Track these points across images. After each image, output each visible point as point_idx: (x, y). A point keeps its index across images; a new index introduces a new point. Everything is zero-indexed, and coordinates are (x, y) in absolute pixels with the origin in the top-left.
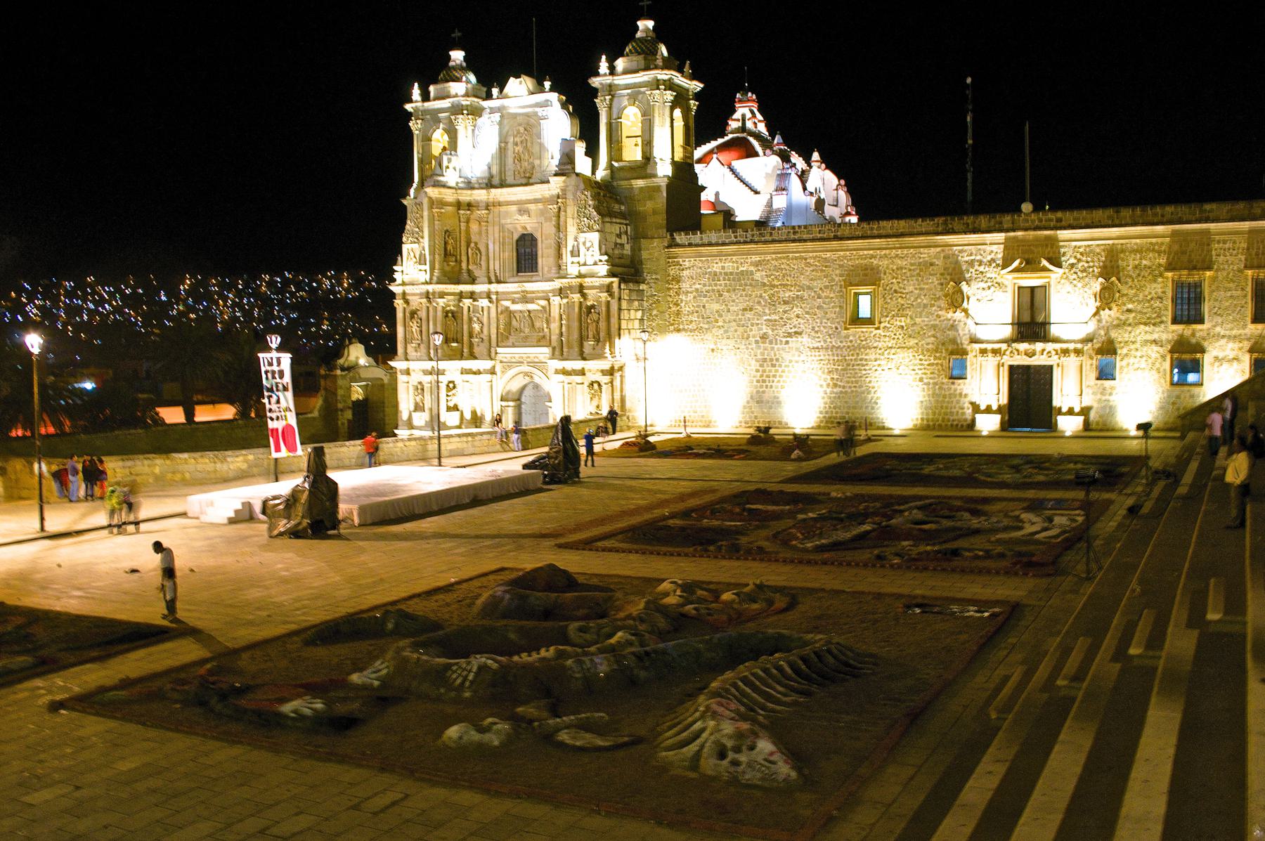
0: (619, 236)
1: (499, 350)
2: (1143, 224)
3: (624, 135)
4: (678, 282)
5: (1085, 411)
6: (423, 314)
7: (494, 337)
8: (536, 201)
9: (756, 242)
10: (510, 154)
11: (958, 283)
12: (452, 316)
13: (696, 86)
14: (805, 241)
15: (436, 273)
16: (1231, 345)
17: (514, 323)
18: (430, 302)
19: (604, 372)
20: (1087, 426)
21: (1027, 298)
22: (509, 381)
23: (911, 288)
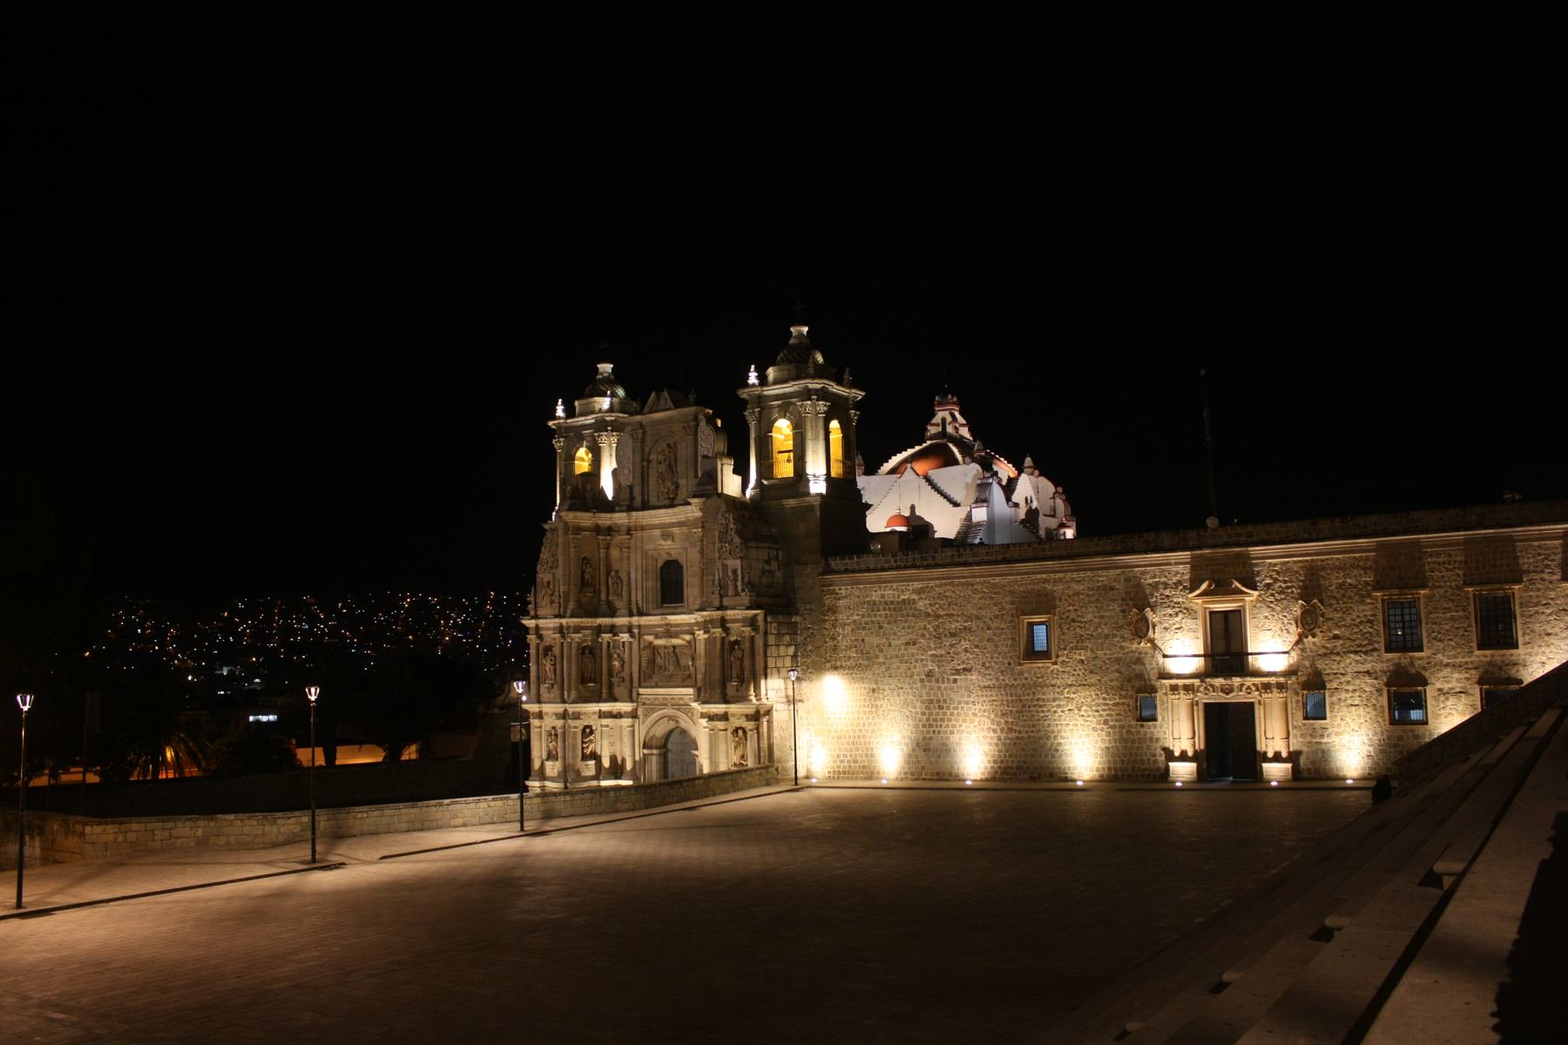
0: (768, 562)
1: (642, 691)
2: (1343, 538)
3: (775, 450)
5: (1293, 757)
6: (556, 651)
7: (635, 676)
8: (680, 524)
9: (917, 567)
11: (1141, 610)
12: (589, 652)
13: (859, 394)
14: (970, 564)
15: (571, 605)
16: (1456, 676)
17: (658, 660)
18: (563, 636)
19: (748, 717)
20: (1296, 772)
21: (1220, 626)
22: (653, 725)
23: (1090, 616)
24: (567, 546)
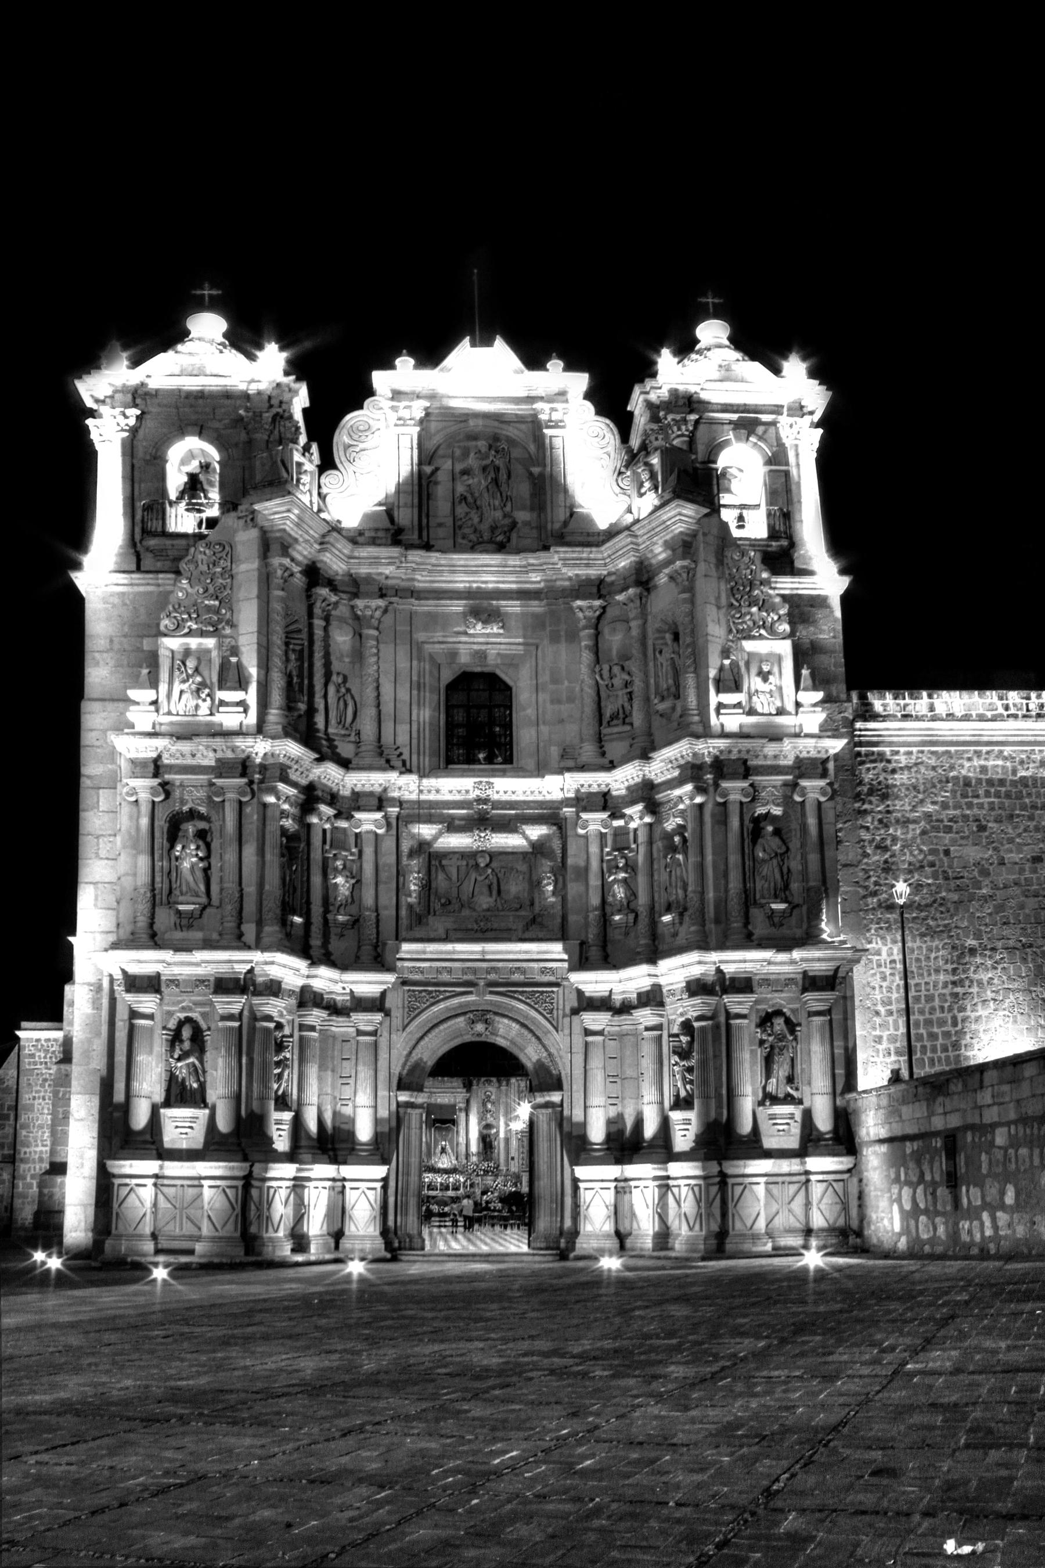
1: (407, 948)
4: (885, 797)
8: (523, 595)
10: (442, 491)
15: (274, 715)
17: (440, 881)
19: (811, 983)
24: (266, 579)
